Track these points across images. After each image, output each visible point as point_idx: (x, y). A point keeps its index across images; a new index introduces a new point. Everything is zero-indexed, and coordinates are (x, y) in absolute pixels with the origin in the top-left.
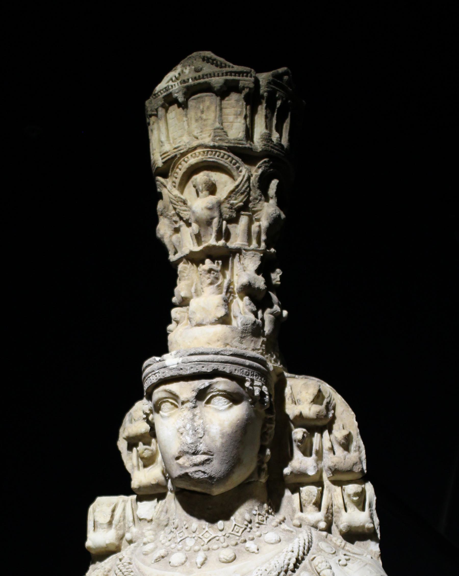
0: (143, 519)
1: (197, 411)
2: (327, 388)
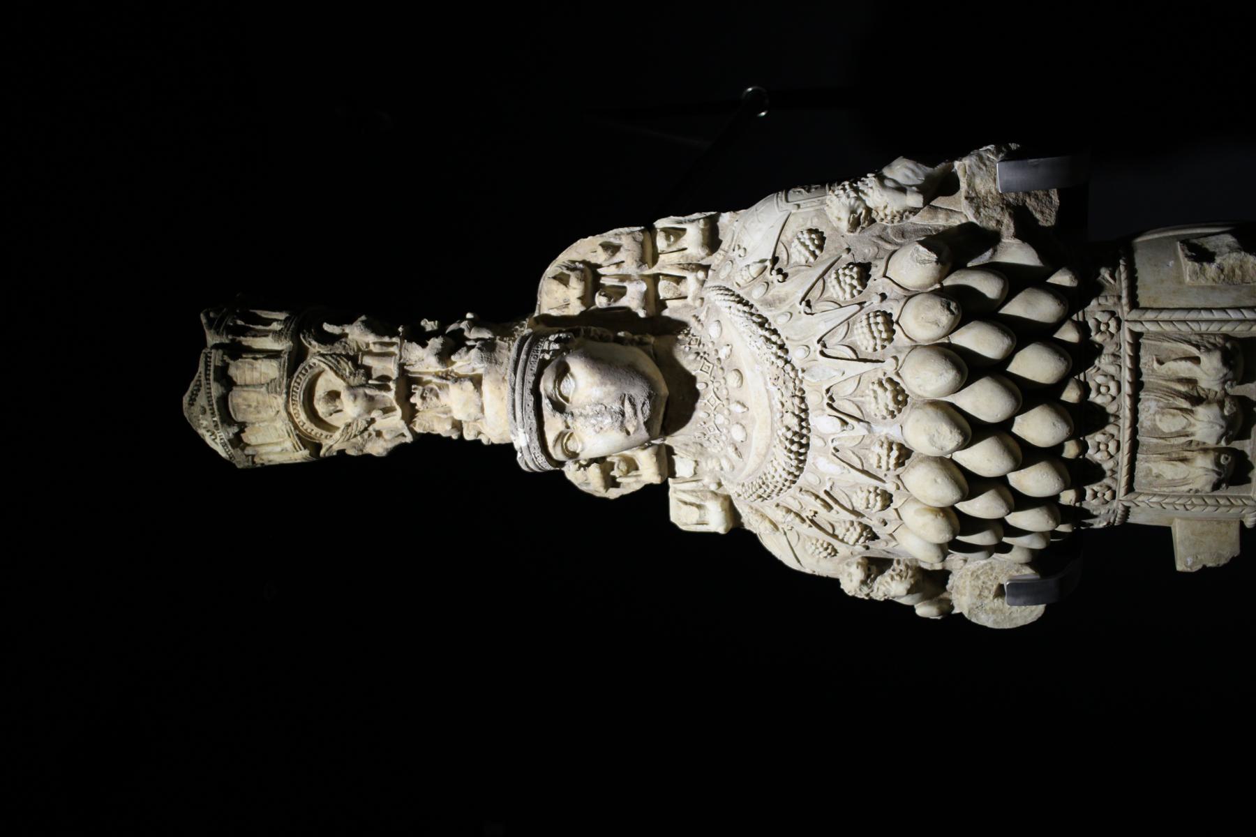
1: (576, 412)
2: (552, 270)
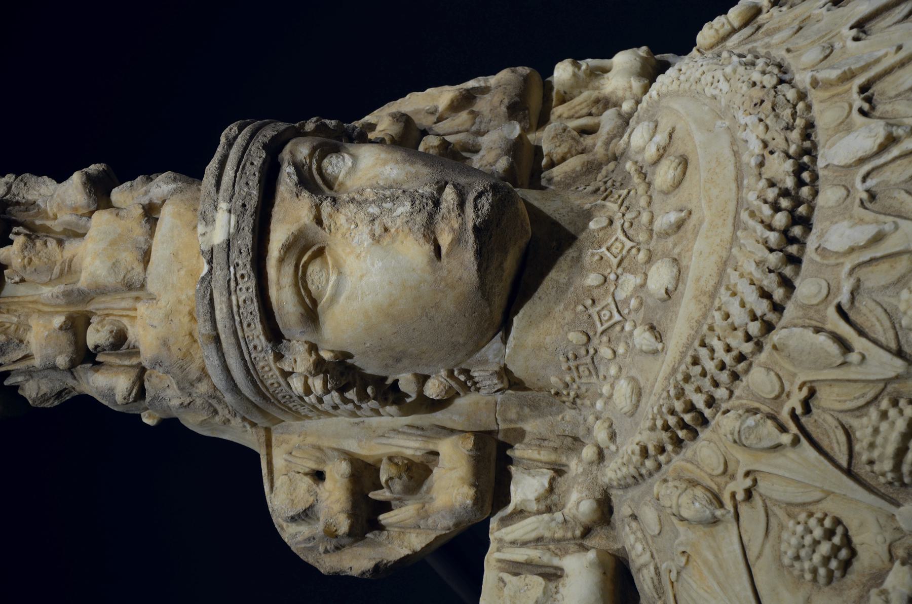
0: (551, 484)
1: (345, 197)
